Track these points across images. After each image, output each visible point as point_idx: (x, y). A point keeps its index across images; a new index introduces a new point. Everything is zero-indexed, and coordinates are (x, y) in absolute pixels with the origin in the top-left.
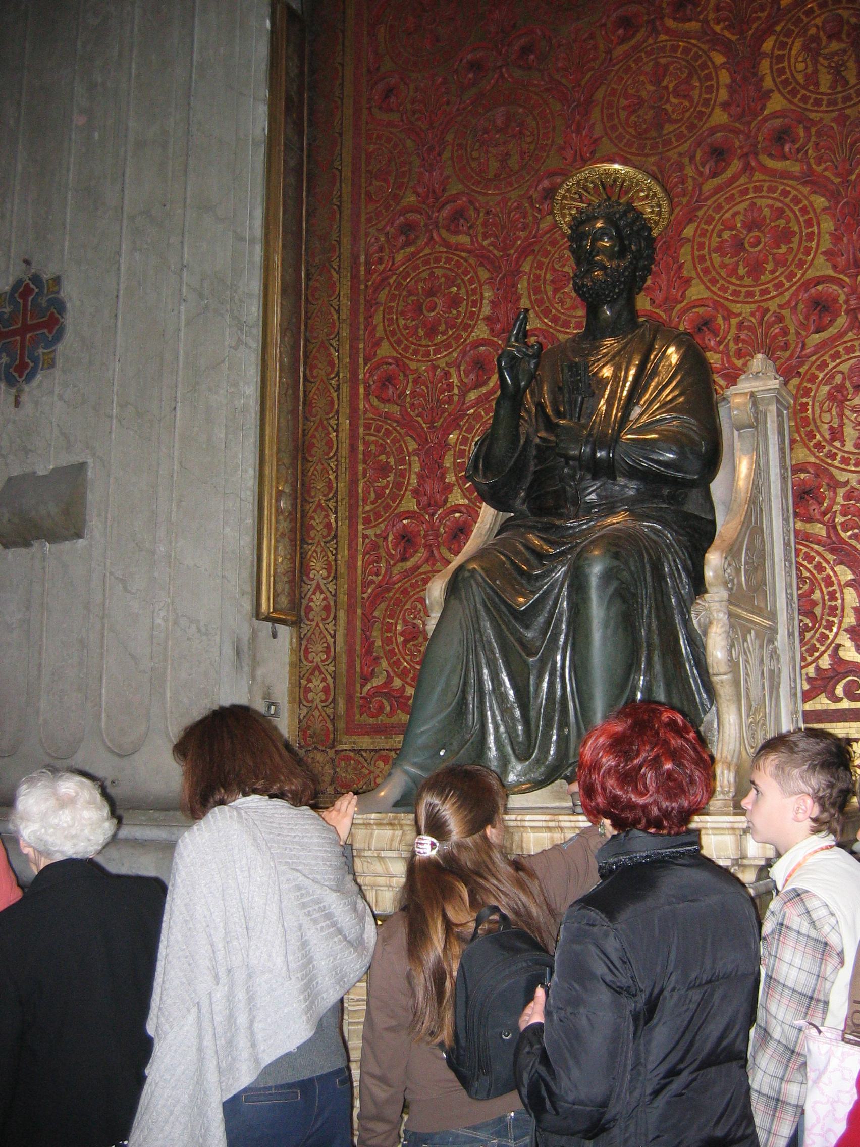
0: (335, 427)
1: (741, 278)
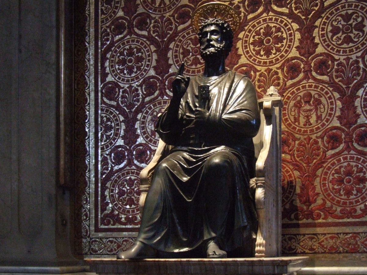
0: (88, 109)
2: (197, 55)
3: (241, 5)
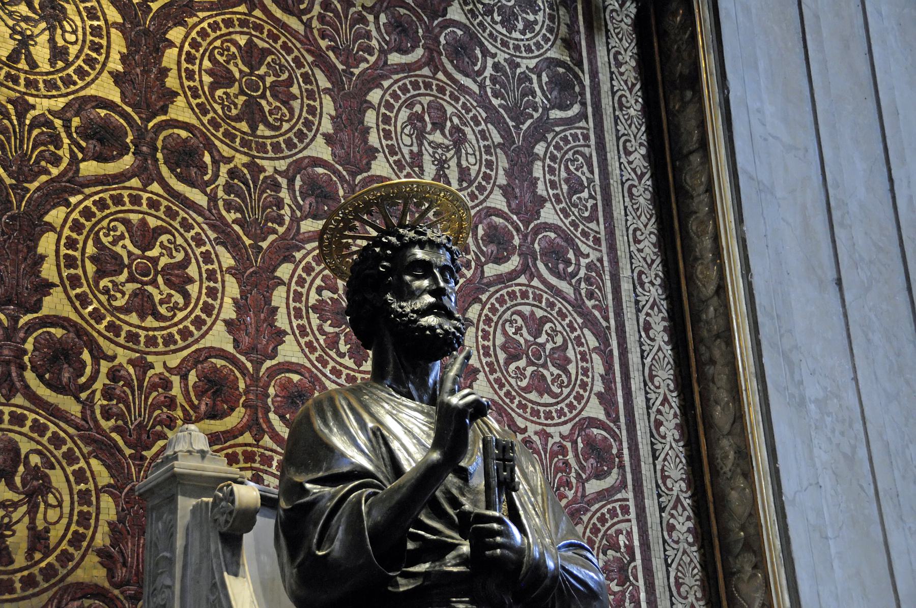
1: (342, 355)
2: (146, 284)
3: (283, 182)
